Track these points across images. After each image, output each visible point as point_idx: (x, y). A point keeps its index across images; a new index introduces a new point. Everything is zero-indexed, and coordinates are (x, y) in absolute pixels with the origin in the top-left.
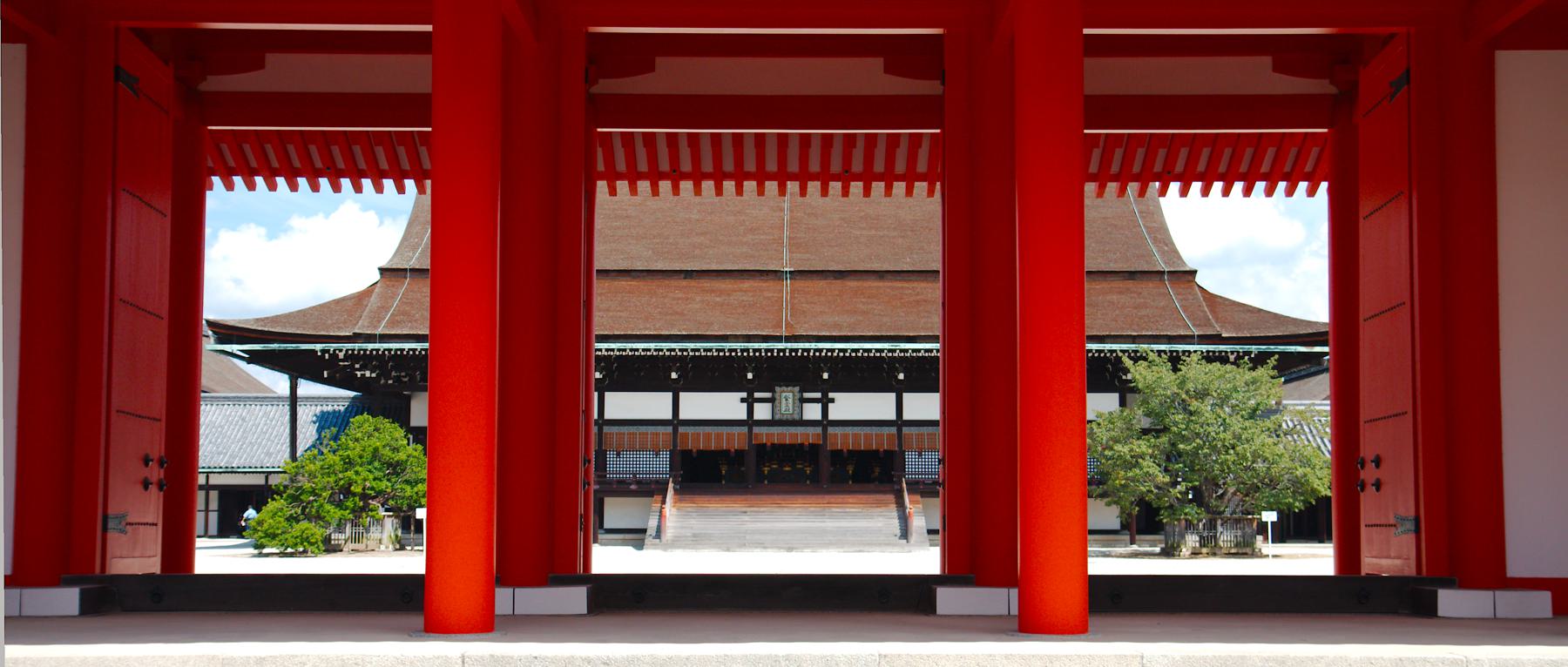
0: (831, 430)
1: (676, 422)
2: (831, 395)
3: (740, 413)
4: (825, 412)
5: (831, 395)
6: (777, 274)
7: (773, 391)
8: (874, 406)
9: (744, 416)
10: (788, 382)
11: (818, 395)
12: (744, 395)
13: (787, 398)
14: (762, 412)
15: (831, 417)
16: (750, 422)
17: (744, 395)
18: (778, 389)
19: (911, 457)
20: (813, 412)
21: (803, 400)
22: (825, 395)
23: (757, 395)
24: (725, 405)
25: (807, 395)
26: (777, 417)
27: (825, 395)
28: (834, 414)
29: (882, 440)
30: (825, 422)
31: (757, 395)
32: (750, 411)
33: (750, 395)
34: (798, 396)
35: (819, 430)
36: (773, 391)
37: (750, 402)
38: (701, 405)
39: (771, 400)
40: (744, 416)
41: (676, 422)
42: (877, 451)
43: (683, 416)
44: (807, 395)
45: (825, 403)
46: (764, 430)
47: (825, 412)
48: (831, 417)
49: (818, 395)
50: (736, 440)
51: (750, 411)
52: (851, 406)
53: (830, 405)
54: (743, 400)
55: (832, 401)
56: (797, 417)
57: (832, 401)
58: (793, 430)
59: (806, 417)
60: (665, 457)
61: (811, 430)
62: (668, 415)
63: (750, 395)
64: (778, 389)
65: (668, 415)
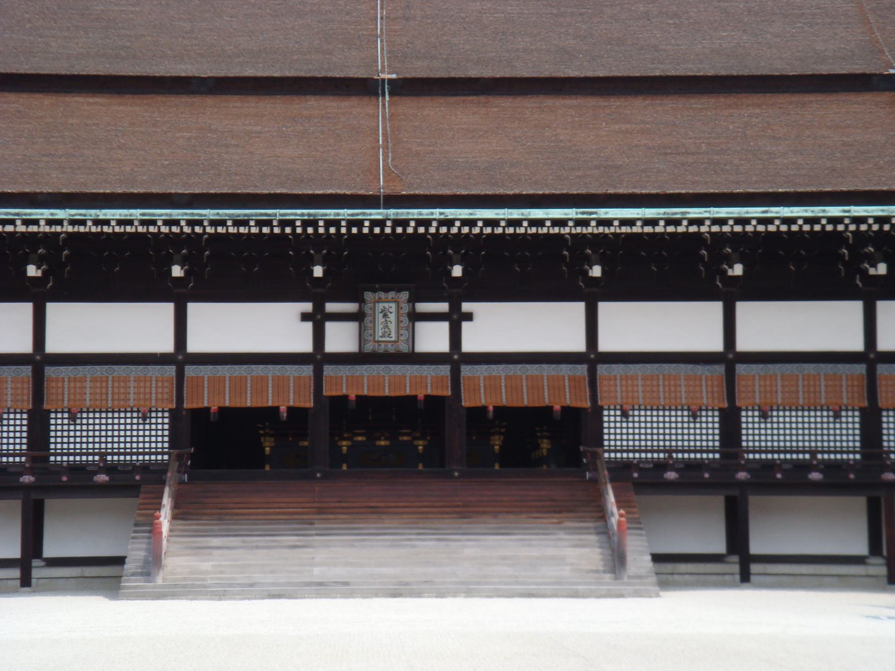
0: (466, 371)
1: (180, 358)
3: (301, 341)
4: (455, 338)
5: (466, 307)
6: (363, 88)
7: (357, 298)
8: (545, 327)
10: (388, 282)
11: (443, 307)
14: (341, 338)
16: (318, 358)
17: (308, 307)
18: (368, 296)
19: (611, 419)
20: (433, 338)
21: (417, 317)
22: (455, 307)
26: (369, 348)
27: (455, 307)
28: (471, 343)
29: (561, 391)
30: (456, 358)
31: (331, 307)
32: (319, 337)
33: (319, 307)
34: (406, 308)
35: (445, 370)
36: (361, 300)
37: (318, 320)
38: (227, 327)
39: (357, 317)
41: (180, 358)
42: (549, 409)
43: (194, 346)
45: (456, 320)
46: (344, 371)
47: (455, 338)
50: (291, 393)
51: (319, 337)
52: (503, 327)
53: (465, 325)
54: (305, 317)
55: (469, 317)
56: (404, 348)
58: (397, 370)
60: (161, 425)
61: (428, 371)
62: (167, 346)
63: (319, 307)
64: (368, 296)
65: (167, 346)
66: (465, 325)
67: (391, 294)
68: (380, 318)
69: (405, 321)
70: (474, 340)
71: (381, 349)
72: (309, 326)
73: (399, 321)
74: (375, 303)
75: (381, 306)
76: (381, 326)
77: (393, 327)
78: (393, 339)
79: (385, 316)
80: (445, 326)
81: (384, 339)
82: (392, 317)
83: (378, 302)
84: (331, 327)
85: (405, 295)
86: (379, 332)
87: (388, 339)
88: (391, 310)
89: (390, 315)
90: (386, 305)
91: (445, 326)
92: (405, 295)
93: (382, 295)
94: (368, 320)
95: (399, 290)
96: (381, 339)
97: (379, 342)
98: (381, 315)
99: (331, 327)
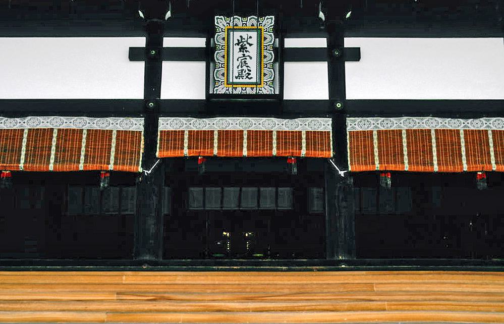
2: (350, 42)
3: (129, 84)
4: (337, 80)
5: (350, 42)
11: (321, 43)
12: (140, 42)
13: (245, 44)
15: (354, 91)
16: (152, 106)
17: (140, 42)
18: (221, 22)
20: (307, 82)
21: (283, 56)
22: (335, 43)
23: (169, 42)
25: (291, 43)
26: (221, 90)
27: (335, 43)
30: (337, 107)
31: (169, 42)
32: (153, 80)
33: (154, 42)
34: (270, 39)
36: (209, 32)
37: (152, 60)
39: (206, 55)
40: (135, 91)
44: (291, 43)
45: (337, 60)
47: (337, 80)
48: (354, 91)
49: (321, 43)
51: (153, 80)
53: (349, 65)
54: (134, 54)
55: (355, 54)
57: (355, 54)
59: (290, 95)
63: (154, 42)
64: (221, 22)
66: (349, 65)
67: (251, 21)
68: (236, 53)
69: (270, 56)
70: (360, 84)
72: (140, 66)
73: (260, 56)
75: (237, 35)
76: (237, 63)
77: (253, 64)
78: (254, 80)
79: (243, 49)
80: (322, 68)
81: (241, 80)
82: (253, 51)
83: (234, 30)
84: (168, 68)
85: (269, 22)
87: (247, 80)
88: (250, 41)
90: (244, 34)
91: (322, 68)
92: (269, 22)
93: (238, 21)
94: (218, 56)
95: (262, 14)
96: (235, 80)
97: (233, 84)
98: (237, 48)
99: (168, 68)
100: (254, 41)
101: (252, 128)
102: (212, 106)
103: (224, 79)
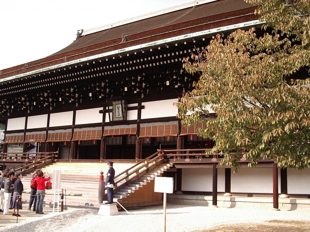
2: (143, 104)
5: (143, 104)
9: (101, 121)
11: (136, 105)
12: (102, 109)
13: (118, 108)
15: (142, 118)
16: (103, 124)
17: (102, 109)
18: (114, 103)
20: (133, 115)
24: (91, 116)
30: (140, 121)
33: (105, 108)
37: (104, 112)
40: (101, 121)
45: (140, 108)
48: (143, 117)
49: (136, 105)
53: (142, 110)
54: (101, 112)
55: (143, 107)
66: (142, 110)
68: (117, 109)
71: (117, 120)
74: (116, 105)
79: (118, 109)
80: (136, 111)
82: (120, 109)
86: (117, 115)
89: (120, 109)
91: (136, 111)
96: (117, 117)
100: (121, 107)
101: (15, 135)
102: (112, 123)
103: (115, 117)
